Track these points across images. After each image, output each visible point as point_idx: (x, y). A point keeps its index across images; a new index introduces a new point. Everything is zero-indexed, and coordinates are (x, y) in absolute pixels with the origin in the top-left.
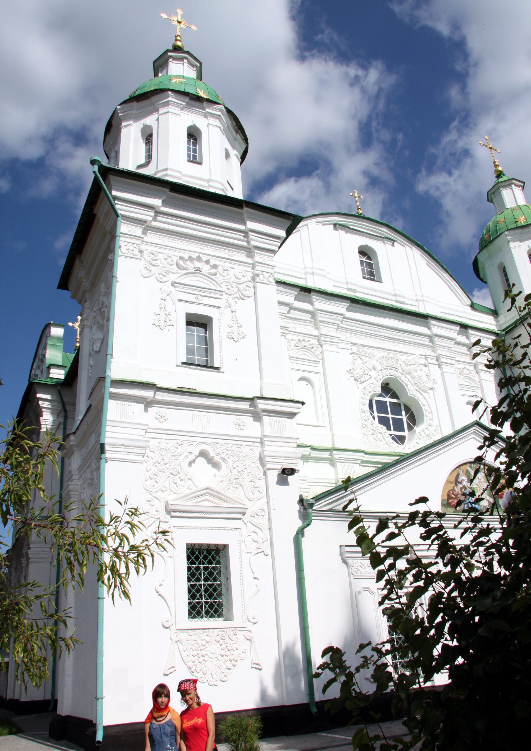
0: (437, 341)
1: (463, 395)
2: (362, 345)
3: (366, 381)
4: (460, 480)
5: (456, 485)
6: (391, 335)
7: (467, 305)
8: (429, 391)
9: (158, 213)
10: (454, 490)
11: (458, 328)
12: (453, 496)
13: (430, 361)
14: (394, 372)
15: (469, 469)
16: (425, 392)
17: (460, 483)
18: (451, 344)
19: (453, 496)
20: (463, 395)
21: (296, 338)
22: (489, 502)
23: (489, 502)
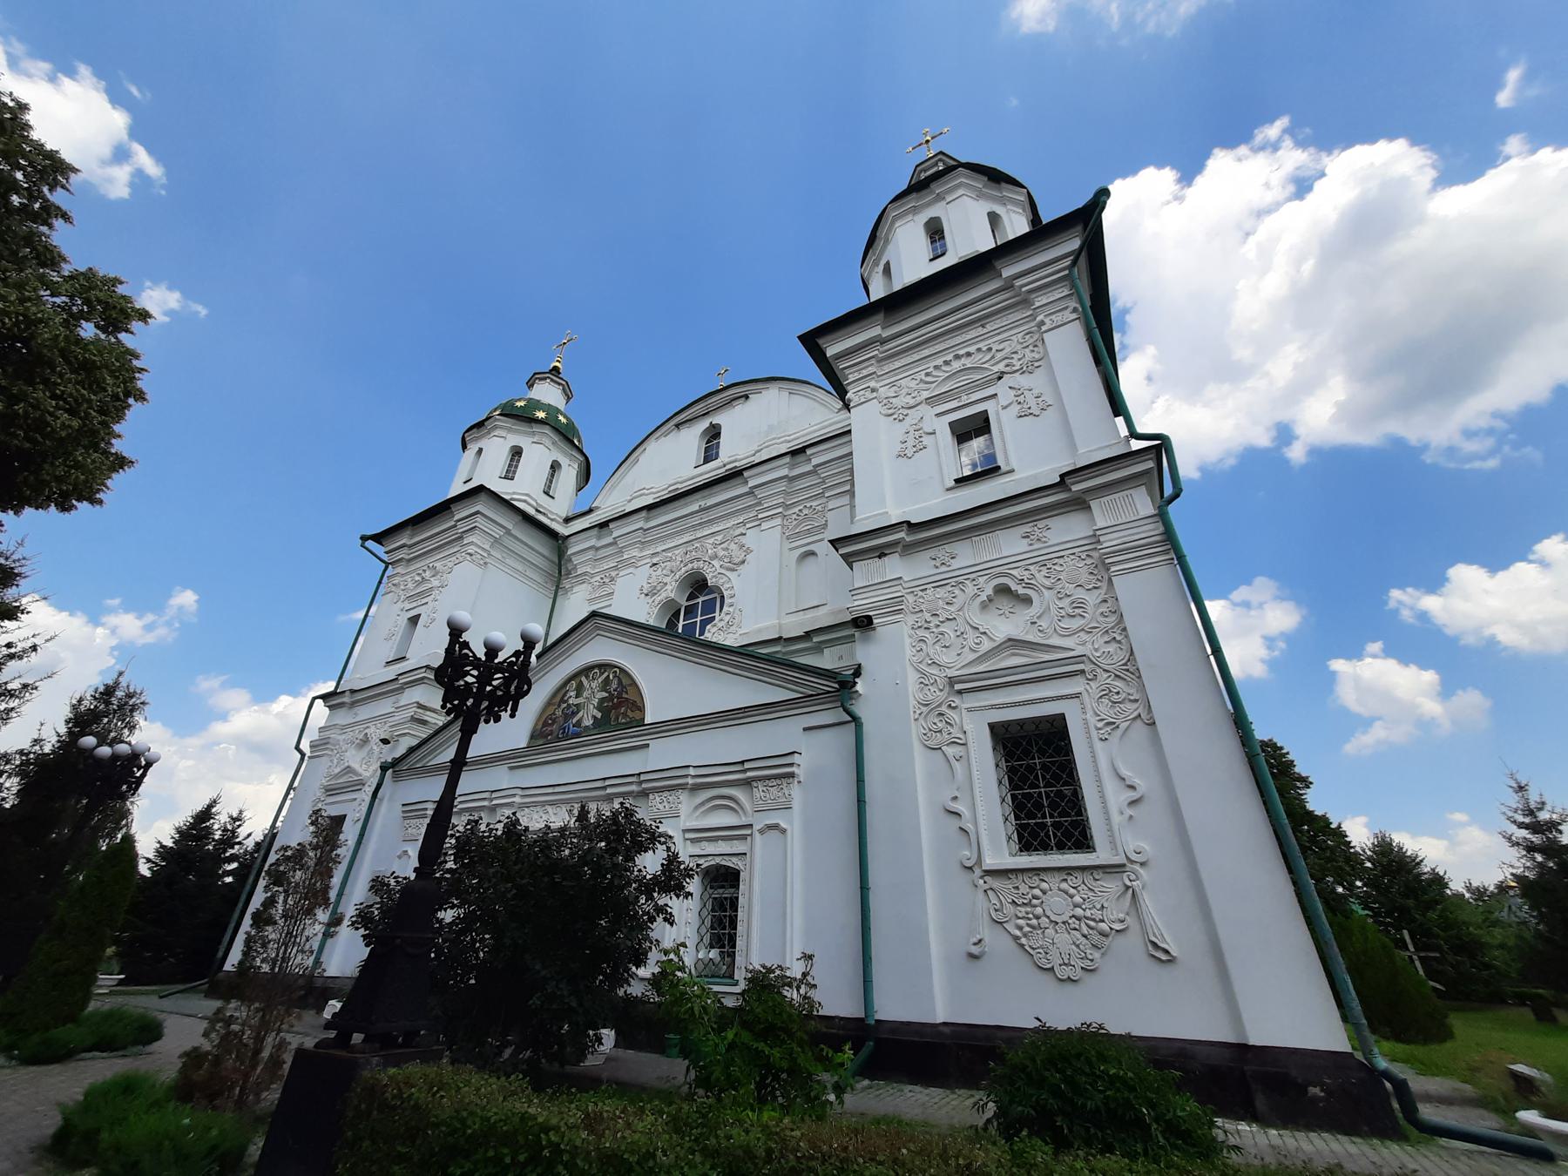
0: (760, 493)
1: (791, 549)
2: (663, 551)
3: (659, 591)
4: (566, 698)
5: (559, 706)
6: (701, 519)
7: (840, 410)
8: (741, 567)
9: (410, 547)
10: (554, 714)
11: (787, 459)
12: (550, 722)
13: (748, 526)
14: (695, 565)
15: (583, 679)
16: (733, 570)
17: (566, 702)
18: (782, 486)
19: (550, 722)
20: (791, 549)
21: (598, 578)
22: (594, 717)
23: (594, 717)
